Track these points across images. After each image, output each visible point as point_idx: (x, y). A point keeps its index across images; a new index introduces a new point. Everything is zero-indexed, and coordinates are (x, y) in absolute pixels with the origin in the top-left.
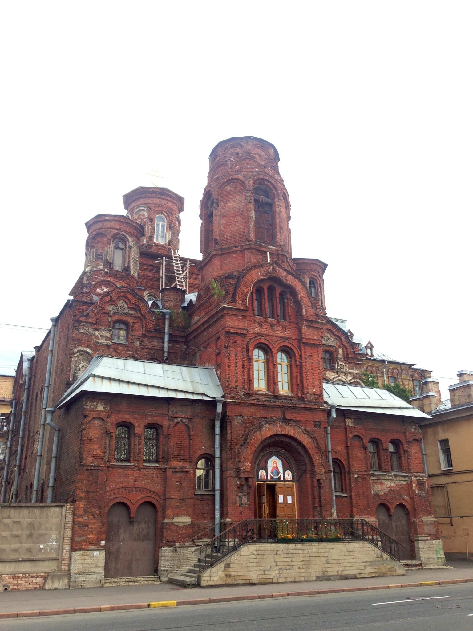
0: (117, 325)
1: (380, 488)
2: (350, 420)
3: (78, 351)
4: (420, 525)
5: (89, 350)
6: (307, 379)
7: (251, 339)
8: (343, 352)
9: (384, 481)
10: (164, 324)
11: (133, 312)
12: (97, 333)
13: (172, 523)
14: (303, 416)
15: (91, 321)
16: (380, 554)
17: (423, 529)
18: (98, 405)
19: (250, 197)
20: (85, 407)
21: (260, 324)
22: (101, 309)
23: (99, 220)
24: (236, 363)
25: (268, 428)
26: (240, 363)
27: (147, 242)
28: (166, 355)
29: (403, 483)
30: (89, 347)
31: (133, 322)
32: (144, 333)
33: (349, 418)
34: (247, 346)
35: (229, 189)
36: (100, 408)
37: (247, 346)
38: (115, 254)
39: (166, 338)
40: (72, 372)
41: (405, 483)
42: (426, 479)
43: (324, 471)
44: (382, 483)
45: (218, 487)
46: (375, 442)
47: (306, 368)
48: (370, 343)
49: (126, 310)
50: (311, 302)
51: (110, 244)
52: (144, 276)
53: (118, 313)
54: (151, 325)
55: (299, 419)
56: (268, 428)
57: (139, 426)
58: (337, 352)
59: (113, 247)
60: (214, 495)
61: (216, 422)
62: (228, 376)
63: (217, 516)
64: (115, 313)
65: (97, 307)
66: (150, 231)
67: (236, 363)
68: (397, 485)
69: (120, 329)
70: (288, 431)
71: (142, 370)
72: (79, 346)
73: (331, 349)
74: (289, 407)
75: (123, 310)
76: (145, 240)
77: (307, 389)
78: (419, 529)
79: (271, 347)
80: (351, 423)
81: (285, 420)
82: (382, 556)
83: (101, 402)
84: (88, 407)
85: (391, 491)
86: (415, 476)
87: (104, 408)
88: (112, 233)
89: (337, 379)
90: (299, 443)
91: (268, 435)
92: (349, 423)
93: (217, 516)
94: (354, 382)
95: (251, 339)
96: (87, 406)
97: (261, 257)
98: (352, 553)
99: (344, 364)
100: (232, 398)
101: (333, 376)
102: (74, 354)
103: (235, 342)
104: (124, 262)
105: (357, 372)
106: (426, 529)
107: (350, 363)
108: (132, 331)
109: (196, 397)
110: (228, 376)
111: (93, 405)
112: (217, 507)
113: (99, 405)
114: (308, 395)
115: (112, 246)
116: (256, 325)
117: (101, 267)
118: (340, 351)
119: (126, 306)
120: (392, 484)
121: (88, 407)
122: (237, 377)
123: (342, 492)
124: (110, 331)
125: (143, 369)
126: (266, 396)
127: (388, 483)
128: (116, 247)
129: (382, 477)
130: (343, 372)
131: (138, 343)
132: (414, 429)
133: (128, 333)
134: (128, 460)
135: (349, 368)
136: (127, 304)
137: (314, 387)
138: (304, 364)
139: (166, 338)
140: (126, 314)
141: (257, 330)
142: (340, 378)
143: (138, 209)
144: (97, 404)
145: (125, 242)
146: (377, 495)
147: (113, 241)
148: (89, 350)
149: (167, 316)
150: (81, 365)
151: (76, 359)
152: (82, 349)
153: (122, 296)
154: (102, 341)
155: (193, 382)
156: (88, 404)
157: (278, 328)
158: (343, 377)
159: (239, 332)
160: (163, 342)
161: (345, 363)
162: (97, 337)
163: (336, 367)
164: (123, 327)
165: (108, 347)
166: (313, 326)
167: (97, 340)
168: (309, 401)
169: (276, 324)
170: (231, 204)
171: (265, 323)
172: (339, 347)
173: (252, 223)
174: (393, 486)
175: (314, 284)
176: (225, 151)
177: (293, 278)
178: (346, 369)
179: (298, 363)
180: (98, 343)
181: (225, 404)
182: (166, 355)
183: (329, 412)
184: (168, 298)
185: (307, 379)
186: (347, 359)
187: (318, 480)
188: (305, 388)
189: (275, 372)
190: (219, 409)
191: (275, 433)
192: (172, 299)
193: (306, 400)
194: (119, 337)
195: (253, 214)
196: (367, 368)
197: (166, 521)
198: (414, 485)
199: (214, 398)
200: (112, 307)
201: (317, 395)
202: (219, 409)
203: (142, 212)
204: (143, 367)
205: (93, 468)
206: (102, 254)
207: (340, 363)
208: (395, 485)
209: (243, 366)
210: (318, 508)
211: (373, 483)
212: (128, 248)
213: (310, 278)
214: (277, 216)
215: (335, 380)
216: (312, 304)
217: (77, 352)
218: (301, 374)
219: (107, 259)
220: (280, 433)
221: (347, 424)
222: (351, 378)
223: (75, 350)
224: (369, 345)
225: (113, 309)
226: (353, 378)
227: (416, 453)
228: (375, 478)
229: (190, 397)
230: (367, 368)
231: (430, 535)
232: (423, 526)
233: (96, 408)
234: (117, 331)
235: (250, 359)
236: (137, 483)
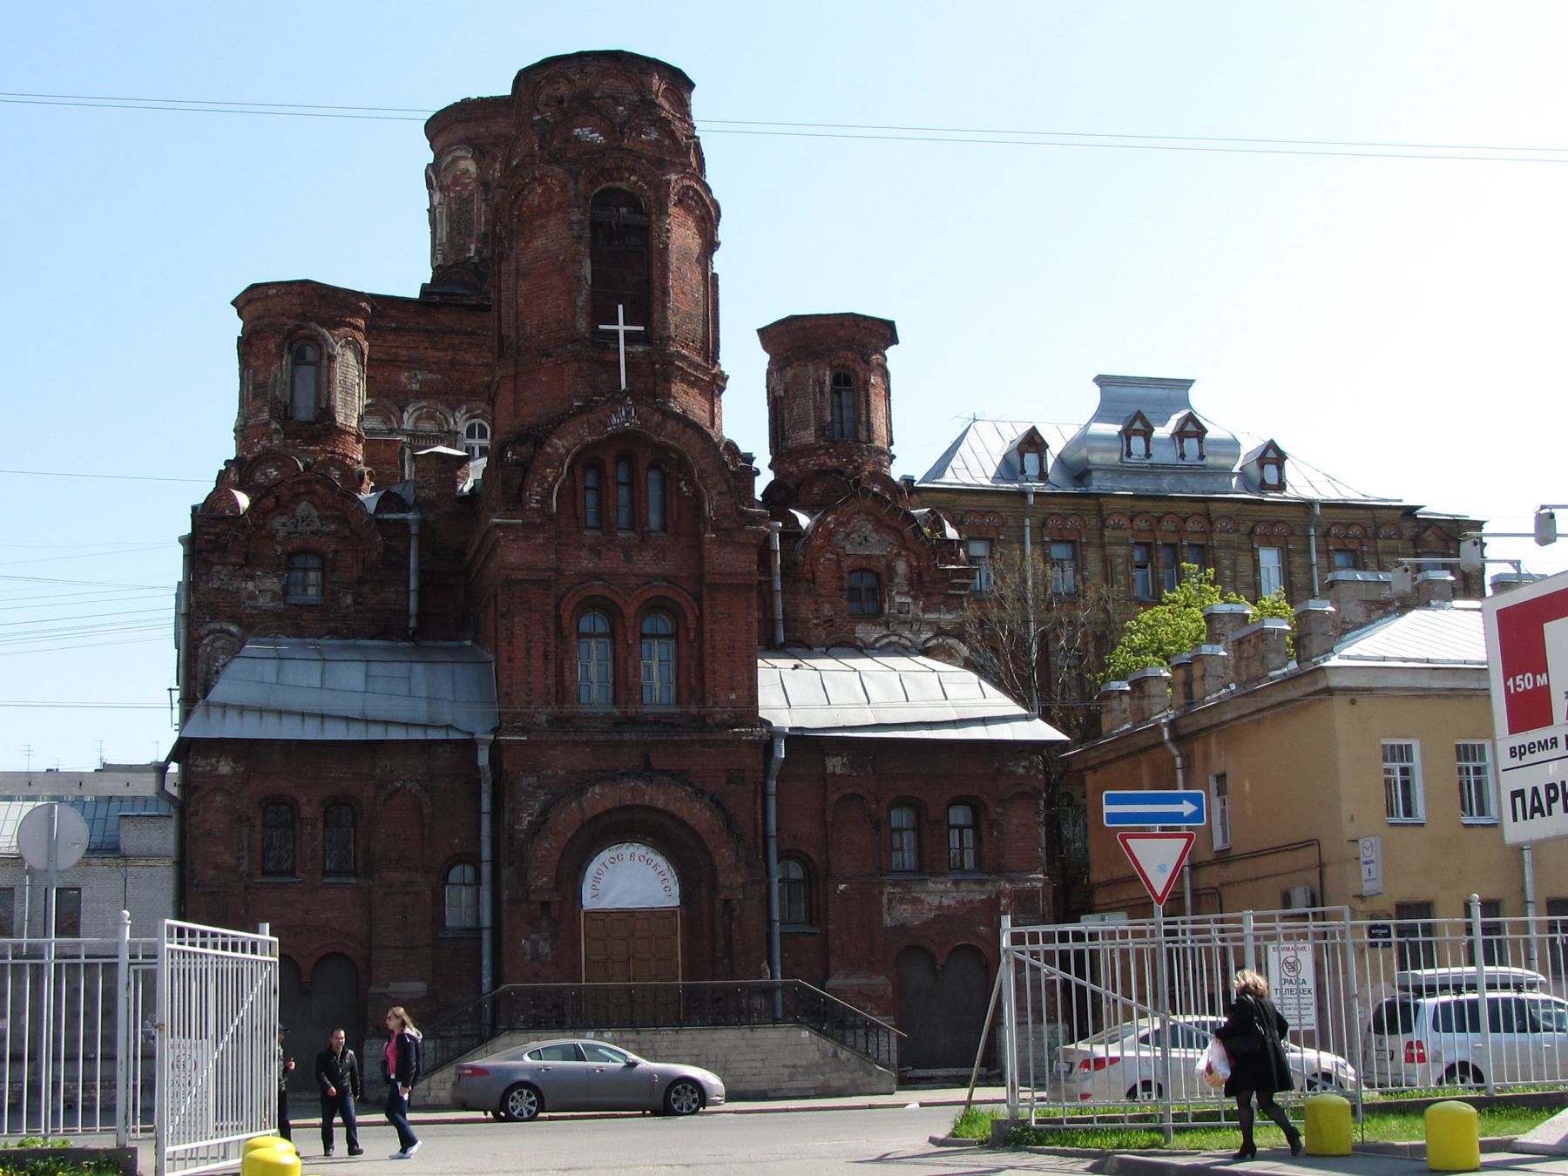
0: (299, 561)
2: (839, 758)
3: (211, 632)
5: (233, 629)
6: (714, 672)
7: (568, 589)
8: (910, 567)
10: (408, 548)
11: (333, 527)
12: (250, 586)
13: (385, 994)
15: (233, 560)
16: (832, 1050)
18: (220, 763)
19: (579, 222)
20: (194, 768)
21: (595, 551)
22: (254, 529)
23: (256, 296)
24: (528, 650)
25: (600, 795)
27: (478, 251)
28: (413, 623)
29: (978, 898)
30: (234, 619)
31: (336, 551)
32: (360, 574)
33: (837, 755)
34: (558, 607)
35: (536, 203)
36: (225, 768)
37: (558, 607)
38: (297, 379)
39: (413, 584)
40: (200, 680)
41: (983, 897)
42: (1040, 885)
43: (740, 881)
44: (919, 899)
45: (486, 920)
46: (915, 805)
47: (713, 647)
48: (1272, 445)
49: (317, 525)
50: (726, 481)
51: (282, 356)
52: (453, 364)
53: (295, 533)
54: (376, 554)
56: (600, 795)
57: (309, 802)
58: (891, 570)
59: (290, 361)
60: (480, 939)
61: (483, 785)
62: (507, 681)
63: (486, 981)
64: (290, 533)
65: (245, 526)
66: (483, 219)
67: (528, 650)
68: (962, 903)
69: (306, 570)
70: (651, 799)
71: (316, 682)
72: (214, 618)
75: (308, 525)
76: (473, 247)
77: (715, 696)
79: (620, 603)
80: (843, 765)
81: (647, 771)
82: (835, 1055)
83: (226, 758)
84: (200, 769)
86: (1011, 881)
87: (233, 769)
88: (286, 327)
89: (886, 640)
90: (682, 822)
91: (600, 809)
92: (835, 765)
93: (486, 981)
94: (938, 646)
95: (568, 589)
96: (198, 766)
97: (604, 376)
98: (758, 1050)
99: (909, 600)
100: (513, 732)
101: (876, 636)
102: (202, 639)
103: (526, 602)
104: (318, 400)
105: (949, 617)
107: (928, 595)
108: (333, 571)
109: (433, 735)
110: (507, 681)
111: (208, 764)
112: (486, 962)
113: (222, 764)
115: (287, 359)
116: (584, 553)
117: (265, 416)
118: (901, 567)
119: (316, 514)
120: (945, 902)
121: (200, 769)
122: (530, 683)
123: (810, 923)
124: (279, 577)
125: (319, 679)
128: (299, 359)
130: (905, 622)
131: (349, 600)
132: (1024, 767)
133: (323, 576)
134: (291, 873)
135: (924, 611)
136: (318, 510)
137: (733, 689)
138: (707, 636)
139: (413, 584)
140: (317, 534)
141: (587, 564)
142: (894, 639)
143: (450, 159)
144: (218, 762)
145: (320, 346)
146: (903, 928)
147: (289, 348)
148: (233, 629)
149: (414, 530)
150: (221, 662)
151: (209, 649)
152: (218, 627)
153: (304, 493)
154: (264, 602)
155: (432, 699)
156: (199, 762)
157: (644, 553)
158: (907, 633)
160: (408, 592)
161: (915, 598)
162: (252, 596)
163: (887, 611)
164: (314, 562)
165: (278, 616)
167: (251, 603)
168: (717, 725)
169: (637, 546)
170: (539, 242)
171: (609, 546)
172: (899, 554)
173: (584, 292)
174: (949, 906)
175: (848, 382)
176: (532, 94)
177: (681, 425)
178: (915, 609)
179: (692, 636)
180: (255, 608)
181: (495, 748)
182: (413, 623)
183: (768, 747)
184: (423, 477)
185: (714, 672)
186: (919, 584)
187: (727, 902)
188: (708, 695)
189: (631, 663)
190: (483, 758)
191: (618, 804)
192: (433, 481)
193: (709, 721)
194: (305, 590)
195: (587, 270)
196: (1252, 531)
197: (373, 990)
198: (1004, 902)
199: (472, 734)
200: (284, 519)
202: (483, 758)
203: (463, 164)
204: (319, 674)
205: (215, 889)
206: (265, 383)
207: (898, 599)
208: (953, 903)
209: (546, 656)
210: (726, 962)
211: (890, 901)
212: (325, 362)
213: (833, 368)
214: (655, 261)
215: (877, 645)
216: (729, 486)
217: (207, 635)
218: (701, 662)
219: (276, 397)
220: (629, 803)
221: (830, 769)
222: (930, 634)
223: (204, 631)
224: (1271, 454)
225: (284, 524)
226: (936, 636)
229: (417, 735)
230: (1252, 531)
233: (216, 770)
234: (300, 575)
235: (566, 637)
236: (310, 917)
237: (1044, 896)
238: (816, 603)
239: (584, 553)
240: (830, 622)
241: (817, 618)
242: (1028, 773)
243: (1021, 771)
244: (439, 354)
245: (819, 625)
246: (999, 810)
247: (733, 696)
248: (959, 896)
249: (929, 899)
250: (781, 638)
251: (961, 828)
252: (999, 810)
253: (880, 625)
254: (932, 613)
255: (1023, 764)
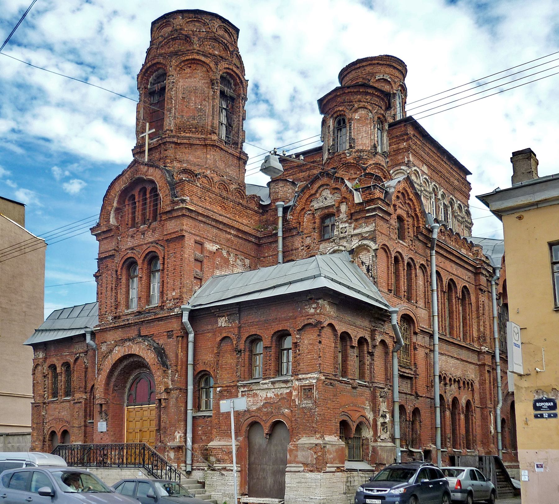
1: (252, 401)
4: (291, 450)
9: (258, 392)
14: (156, 328)
17: (296, 456)
26: (109, 289)
41: (288, 391)
42: (314, 381)
55: (153, 333)
67: (107, 288)
68: (276, 395)
73: (331, 210)
74: (142, 321)
78: (290, 456)
85: (268, 403)
86: (297, 380)
106: (301, 455)
114: (168, 301)
116: (129, 239)
120: (269, 395)
126: (132, 315)
127: (263, 394)
129: (255, 387)
132: (313, 308)
137: (174, 290)
159: (108, 255)
166: (173, 217)
174: (271, 398)
185: (168, 283)
198: (294, 393)
201: (177, 299)
208: (272, 395)
227: (310, 344)
228: (246, 389)
231: (306, 465)
232: (297, 451)
237: (316, 389)
238: (302, 238)
239: (129, 238)
240: (308, 247)
241: (303, 246)
242: (316, 311)
243: (312, 311)
244: (304, 174)
245: (303, 249)
246: (298, 336)
247: (174, 294)
248: (276, 391)
249: (261, 394)
250: (280, 260)
251: (288, 349)
252: (298, 336)
253: (332, 242)
254: (358, 229)
255: (313, 306)
